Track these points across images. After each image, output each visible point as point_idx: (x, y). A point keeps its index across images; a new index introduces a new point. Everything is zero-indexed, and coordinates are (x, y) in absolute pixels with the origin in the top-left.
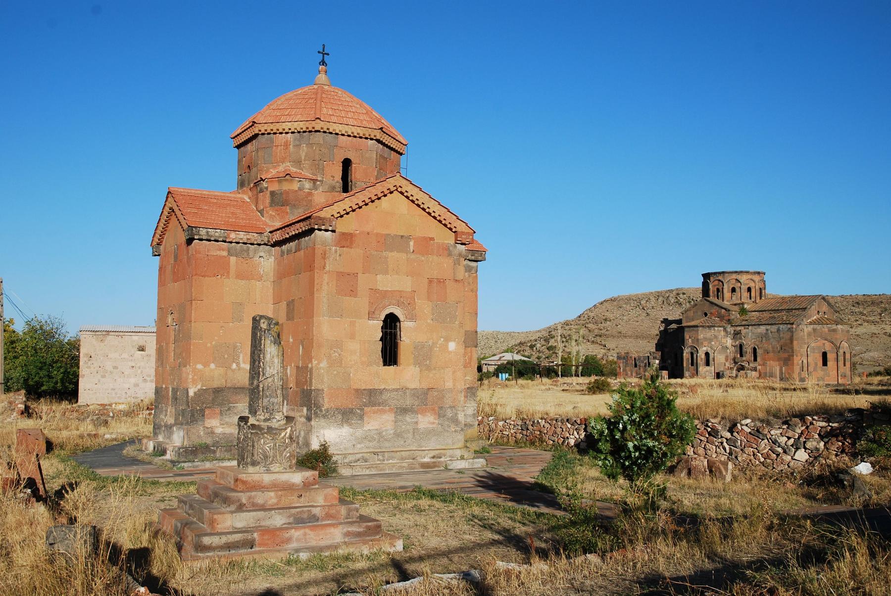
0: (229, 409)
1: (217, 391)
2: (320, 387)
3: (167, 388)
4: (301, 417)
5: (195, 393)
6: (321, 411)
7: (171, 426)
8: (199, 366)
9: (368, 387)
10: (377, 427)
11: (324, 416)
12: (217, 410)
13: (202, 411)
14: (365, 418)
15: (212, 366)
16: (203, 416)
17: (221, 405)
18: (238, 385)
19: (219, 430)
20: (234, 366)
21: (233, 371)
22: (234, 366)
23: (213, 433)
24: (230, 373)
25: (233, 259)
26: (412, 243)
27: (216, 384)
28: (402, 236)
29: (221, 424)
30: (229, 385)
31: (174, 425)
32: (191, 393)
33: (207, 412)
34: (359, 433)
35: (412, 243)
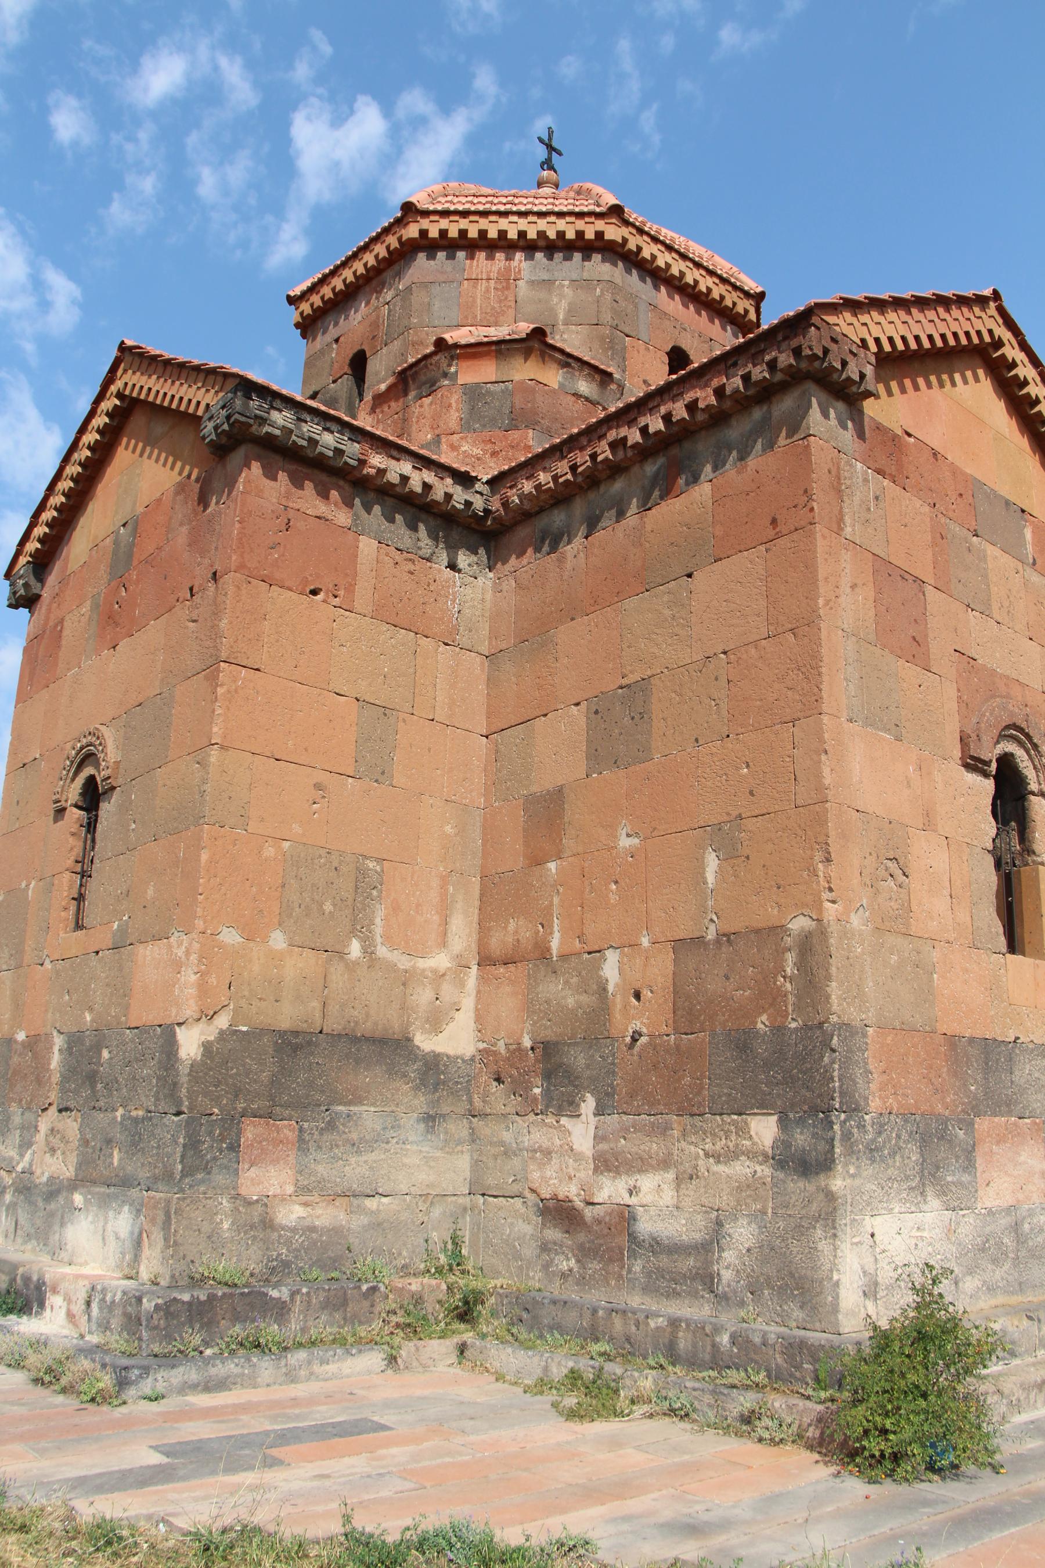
0: (331, 1126)
1: (293, 1045)
2: (854, 1015)
3: (36, 1044)
4: (731, 1155)
5: (207, 1046)
6: (861, 1127)
7: (54, 1190)
8: (230, 937)
9: (978, 1034)
10: (1008, 1200)
11: (872, 1150)
12: (287, 1130)
13: (232, 1122)
14: (979, 1162)
15: (278, 940)
16: (235, 1147)
17: (302, 1106)
18: (366, 1028)
19: (292, 1214)
20: (355, 949)
21: (352, 967)
22: (355, 949)
23: (267, 1224)
24: (338, 976)
25: (367, 546)
26: (1028, 534)
27: (286, 1016)
28: (1007, 503)
29: (302, 1190)
30: (333, 1025)
31: (74, 1185)
32: (190, 1043)
33: (251, 1131)
34: (968, 1226)
35: (1028, 534)
